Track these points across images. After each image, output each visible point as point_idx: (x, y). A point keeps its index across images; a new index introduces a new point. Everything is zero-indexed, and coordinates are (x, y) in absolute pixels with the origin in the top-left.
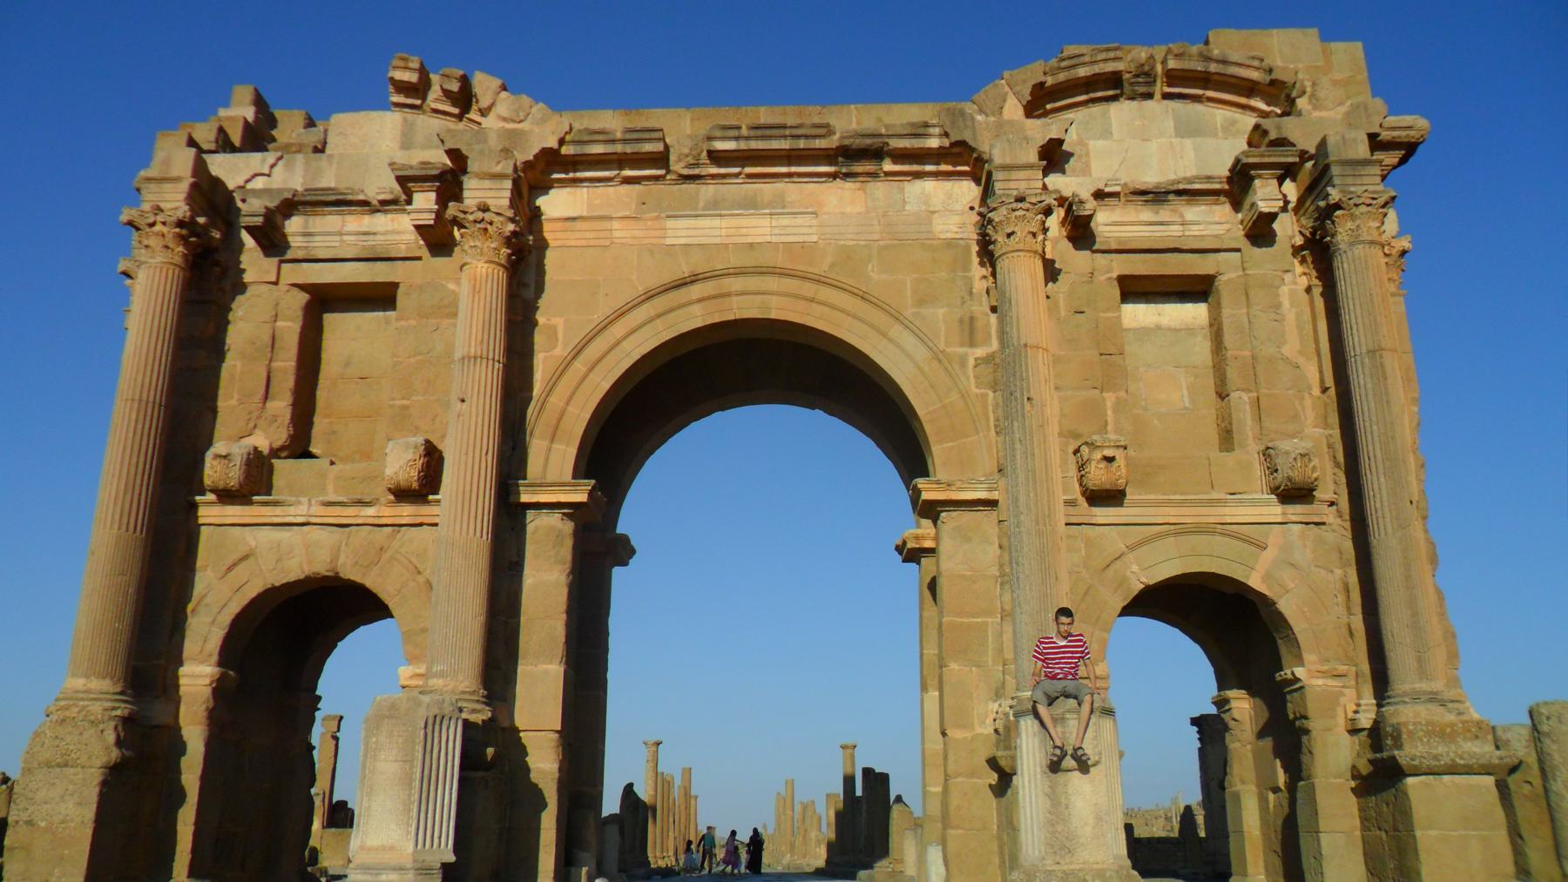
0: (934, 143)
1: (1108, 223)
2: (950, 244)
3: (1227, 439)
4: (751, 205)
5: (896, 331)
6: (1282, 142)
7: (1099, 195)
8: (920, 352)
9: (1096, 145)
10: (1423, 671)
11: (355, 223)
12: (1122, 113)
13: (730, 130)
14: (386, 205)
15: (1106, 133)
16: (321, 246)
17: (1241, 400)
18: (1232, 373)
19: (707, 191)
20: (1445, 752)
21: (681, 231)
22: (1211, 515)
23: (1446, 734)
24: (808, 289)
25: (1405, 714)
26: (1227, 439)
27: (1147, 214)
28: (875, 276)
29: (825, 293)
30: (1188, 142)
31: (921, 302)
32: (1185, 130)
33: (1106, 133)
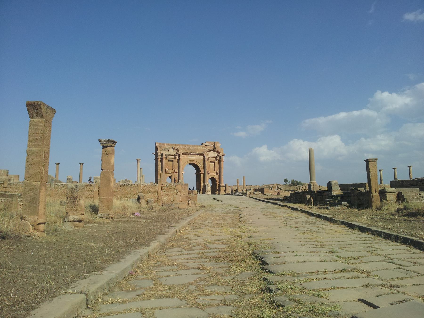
0: (202, 154)
1: (210, 159)
2: (202, 159)
3: (214, 170)
4: (192, 156)
5: (199, 164)
6: (219, 155)
7: (210, 157)
8: (200, 165)
9: (209, 154)
10: (222, 182)
11: (171, 156)
12: (211, 151)
13: (191, 153)
14: (173, 155)
15: (210, 153)
16: (169, 157)
17: (215, 168)
18: (215, 167)
19: (190, 155)
20: (222, 186)
21: (189, 158)
22: (213, 175)
23: (222, 185)
24: (195, 162)
25: (220, 184)
26: (214, 170)
27: (212, 158)
28: (198, 161)
29: (196, 162)
30: (214, 154)
31: (200, 162)
32: (214, 153)
33: (210, 153)
